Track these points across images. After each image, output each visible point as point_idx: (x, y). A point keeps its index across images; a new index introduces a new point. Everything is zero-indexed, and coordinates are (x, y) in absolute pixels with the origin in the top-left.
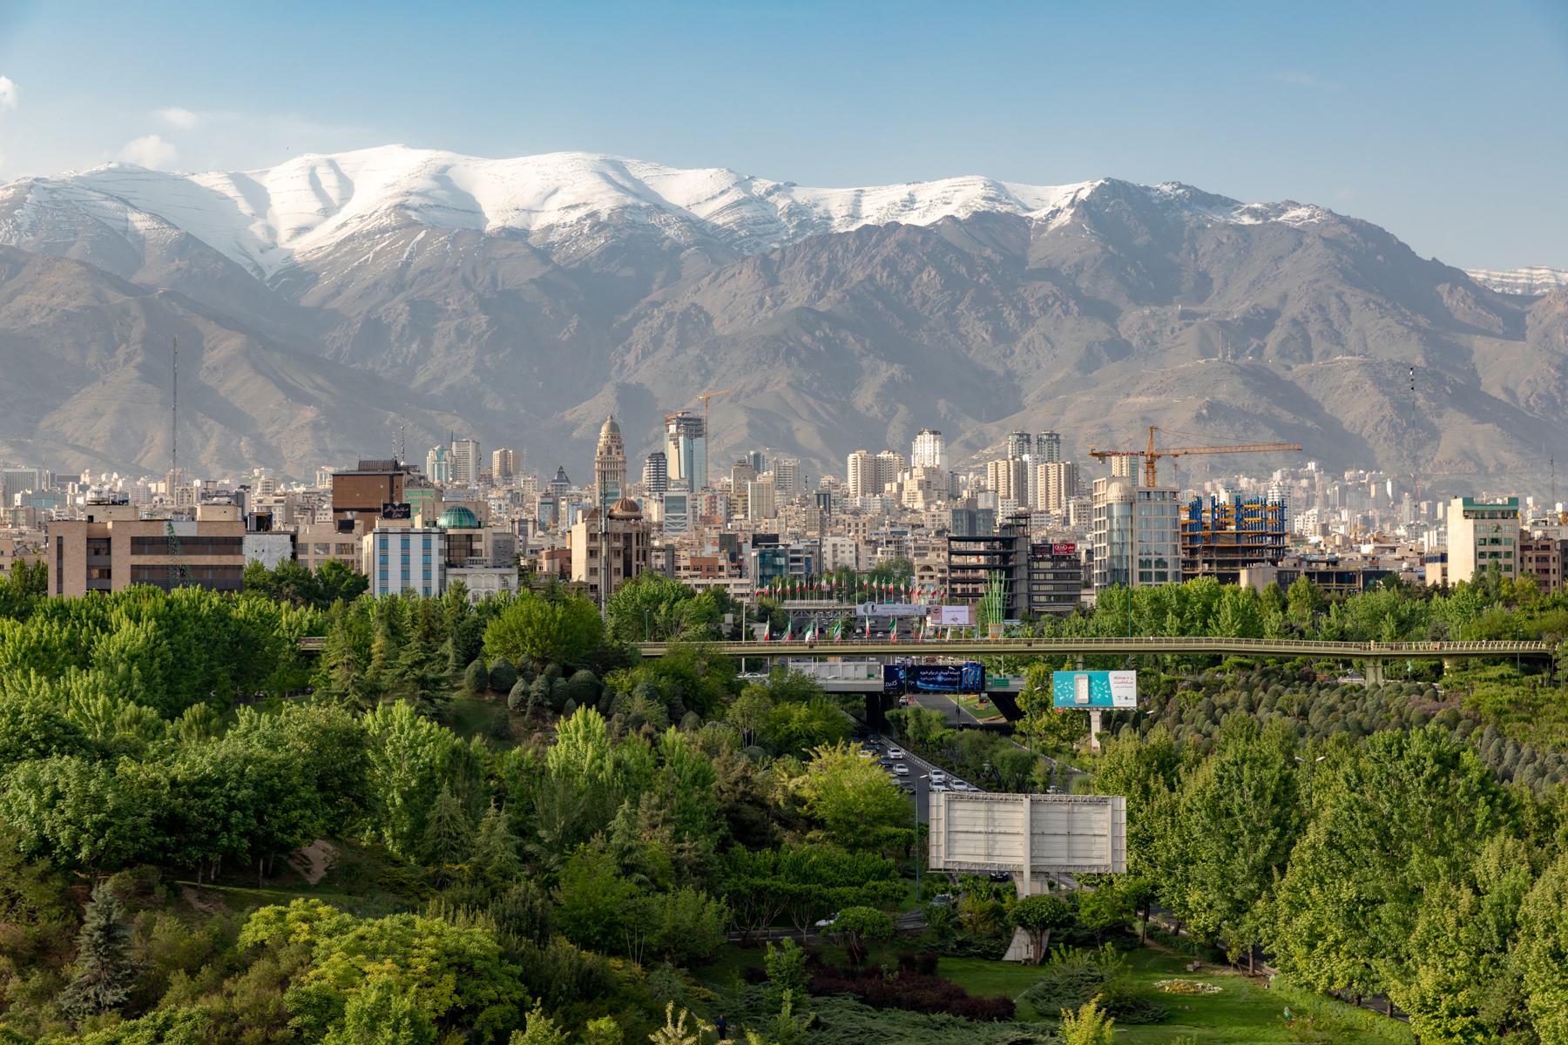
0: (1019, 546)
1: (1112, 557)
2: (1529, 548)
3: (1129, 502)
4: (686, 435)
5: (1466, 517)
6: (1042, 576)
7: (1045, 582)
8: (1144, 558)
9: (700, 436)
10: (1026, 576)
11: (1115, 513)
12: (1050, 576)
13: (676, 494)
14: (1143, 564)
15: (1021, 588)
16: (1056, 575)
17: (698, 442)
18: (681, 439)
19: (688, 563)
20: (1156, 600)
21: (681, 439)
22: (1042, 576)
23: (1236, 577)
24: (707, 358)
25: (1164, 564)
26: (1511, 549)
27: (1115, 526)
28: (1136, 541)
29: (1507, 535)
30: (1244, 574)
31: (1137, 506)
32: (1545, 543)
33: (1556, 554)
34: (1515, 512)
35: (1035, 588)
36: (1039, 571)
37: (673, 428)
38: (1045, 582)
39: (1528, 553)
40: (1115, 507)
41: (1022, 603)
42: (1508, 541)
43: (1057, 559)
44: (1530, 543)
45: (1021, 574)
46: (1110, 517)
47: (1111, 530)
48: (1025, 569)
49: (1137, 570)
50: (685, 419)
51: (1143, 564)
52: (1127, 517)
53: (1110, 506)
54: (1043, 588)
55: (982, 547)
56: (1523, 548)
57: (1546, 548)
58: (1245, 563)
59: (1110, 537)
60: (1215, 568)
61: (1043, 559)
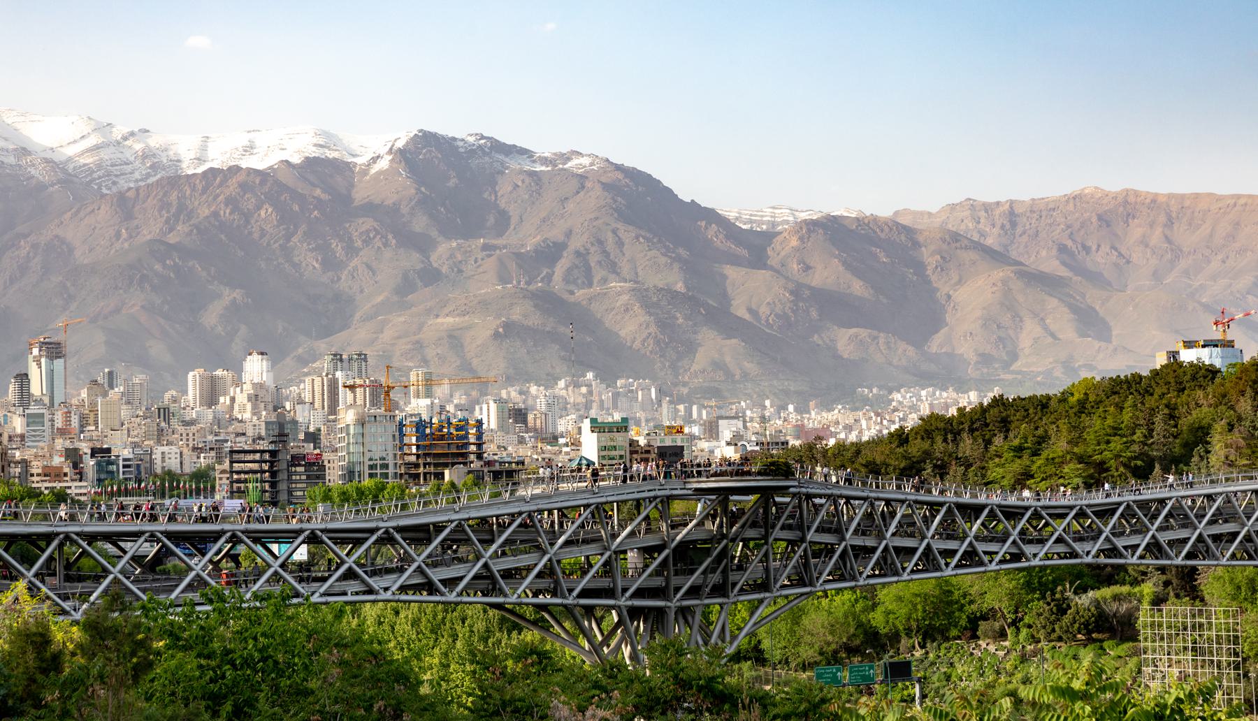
0: (280, 456)
1: (349, 462)
2: (636, 452)
3: (361, 422)
4: (47, 357)
5: (593, 431)
6: (298, 477)
7: (300, 481)
8: (371, 463)
9: (60, 357)
10: (286, 477)
11: (352, 431)
12: (304, 477)
13: (36, 411)
14: (371, 467)
15: (283, 486)
16: (308, 477)
17: (59, 363)
18: (43, 360)
19: (40, 471)
20: (344, 493)
21: (43, 360)
22: (298, 477)
23: (443, 474)
24: (69, 284)
25: (386, 466)
26: (623, 453)
27: (351, 441)
28: (366, 451)
29: (620, 444)
30: (447, 472)
31: (367, 426)
32: (648, 449)
33: (653, 456)
34: (626, 428)
35: (294, 486)
36: (296, 473)
37: (36, 351)
38: (300, 481)
39: (635, 456)
40: (352, 428)
41: (283, 497)
42: (622, 448)
43: (309, 465)
44: (638, 448)
45: (283, 476)
46: (348, 434)
47: (349, 444)
48: (286, 474)
49: (367, 472)
50: (46, 343)
51: (371, 467)
52: (359, 434)
53: (348, 425)
54: (298, 485)
55: (257, 456)
56: (632, 453)
57: (648, 452)
58: (446, 465)
59: (348, 448)
60: (432, 469)
61: (300, 465)
